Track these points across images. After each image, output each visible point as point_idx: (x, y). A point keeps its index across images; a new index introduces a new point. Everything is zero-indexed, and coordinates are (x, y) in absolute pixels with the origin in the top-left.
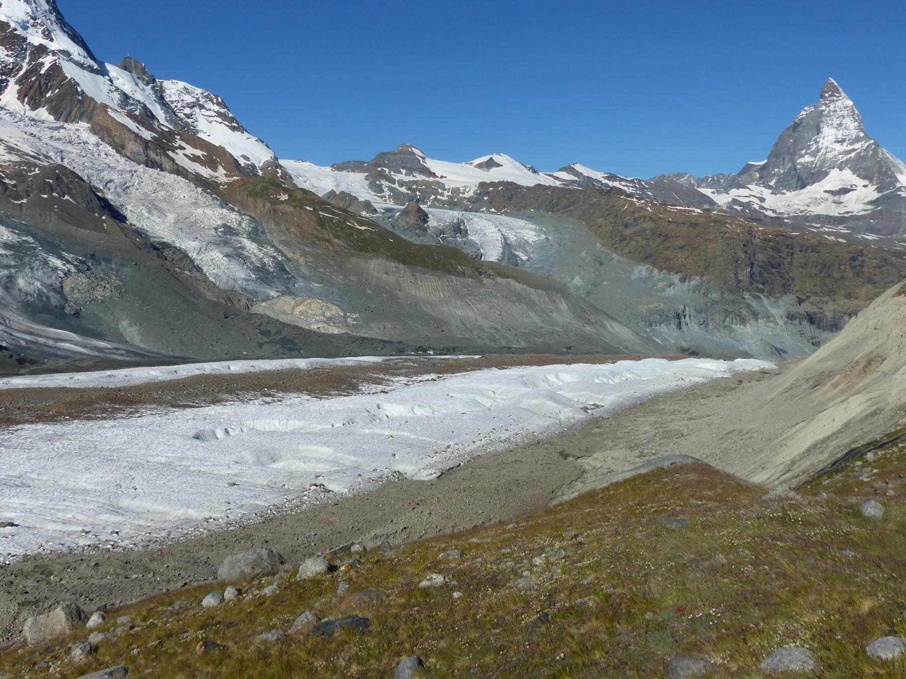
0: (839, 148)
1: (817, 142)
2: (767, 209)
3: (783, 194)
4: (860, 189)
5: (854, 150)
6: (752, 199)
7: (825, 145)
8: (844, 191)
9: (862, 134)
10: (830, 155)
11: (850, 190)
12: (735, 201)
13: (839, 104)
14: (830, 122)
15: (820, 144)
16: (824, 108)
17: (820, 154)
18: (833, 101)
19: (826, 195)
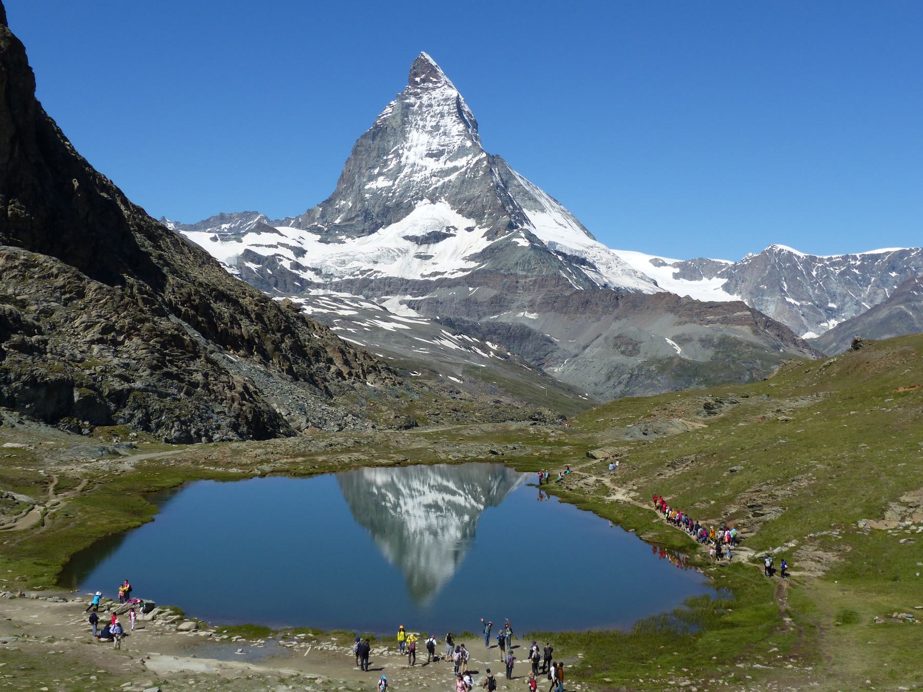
0: (433, 165)
1: (398, 156)
2: (305, 269)
3: (341, 242)
4: (461, 233)
5: (455, 169)
6: (281, 251)
7: (410, 161)
8: (436, 237)
9: (469, 144)
10: (417, 178)
11: (445, 236)
12: (249, 255)
13: (436, 94)
14: (421, 123)
15: (403, 159)
16: (412, 100)
17: (402, 175)
18: (427, 89)
19: (408, 243)
